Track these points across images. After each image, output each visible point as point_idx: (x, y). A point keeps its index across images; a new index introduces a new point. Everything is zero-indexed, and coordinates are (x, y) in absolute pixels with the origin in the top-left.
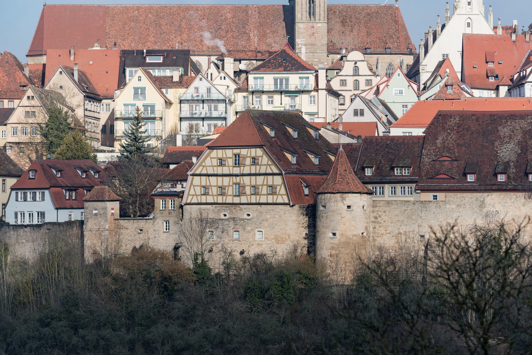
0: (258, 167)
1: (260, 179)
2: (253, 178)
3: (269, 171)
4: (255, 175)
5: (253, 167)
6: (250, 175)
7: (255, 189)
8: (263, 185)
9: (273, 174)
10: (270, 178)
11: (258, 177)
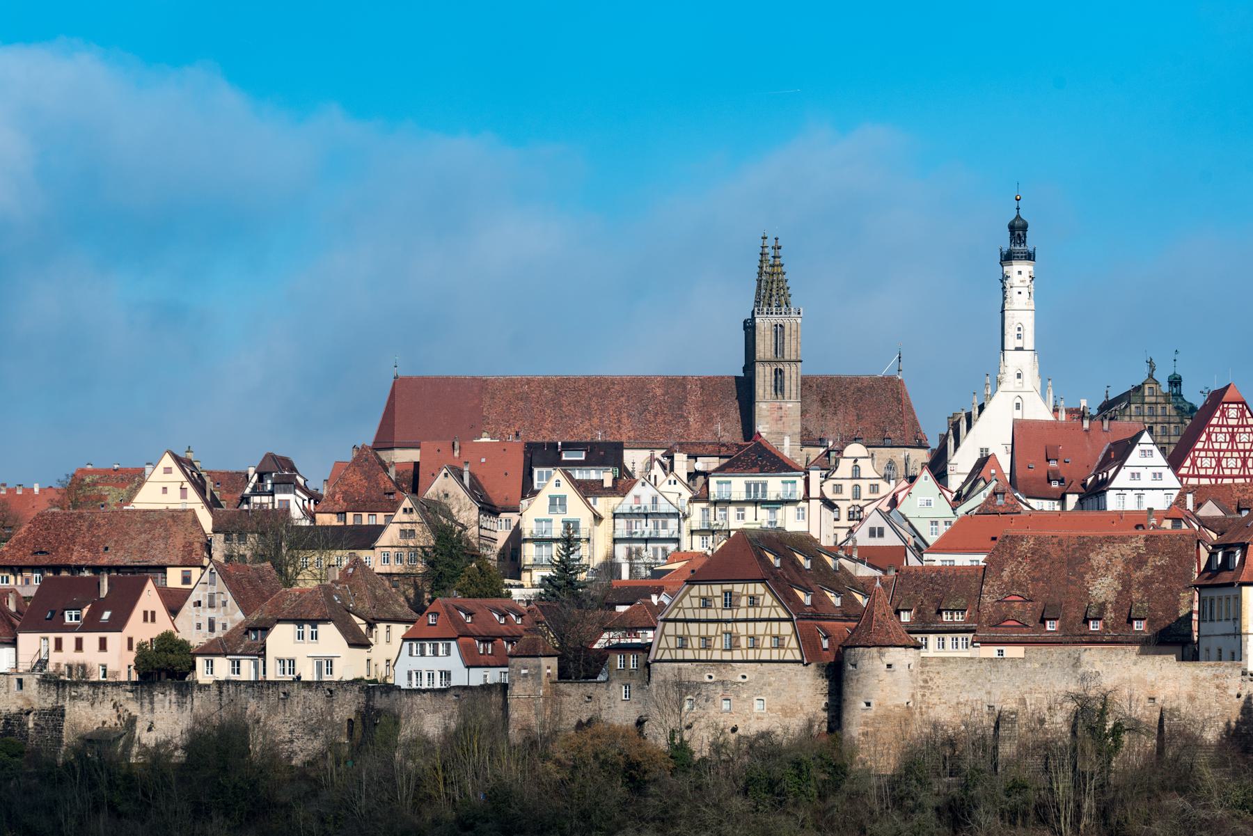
0: (758, 610)
1: (761, 627)
2: (751, 625)
3: (774, 615)
4: (754, 620)
5: (751, 610)
6: (746, 620)
7: (754, 641)
8: (764, 635)
9: (780, 620)
10: (775, 624)
11: (758, 624)
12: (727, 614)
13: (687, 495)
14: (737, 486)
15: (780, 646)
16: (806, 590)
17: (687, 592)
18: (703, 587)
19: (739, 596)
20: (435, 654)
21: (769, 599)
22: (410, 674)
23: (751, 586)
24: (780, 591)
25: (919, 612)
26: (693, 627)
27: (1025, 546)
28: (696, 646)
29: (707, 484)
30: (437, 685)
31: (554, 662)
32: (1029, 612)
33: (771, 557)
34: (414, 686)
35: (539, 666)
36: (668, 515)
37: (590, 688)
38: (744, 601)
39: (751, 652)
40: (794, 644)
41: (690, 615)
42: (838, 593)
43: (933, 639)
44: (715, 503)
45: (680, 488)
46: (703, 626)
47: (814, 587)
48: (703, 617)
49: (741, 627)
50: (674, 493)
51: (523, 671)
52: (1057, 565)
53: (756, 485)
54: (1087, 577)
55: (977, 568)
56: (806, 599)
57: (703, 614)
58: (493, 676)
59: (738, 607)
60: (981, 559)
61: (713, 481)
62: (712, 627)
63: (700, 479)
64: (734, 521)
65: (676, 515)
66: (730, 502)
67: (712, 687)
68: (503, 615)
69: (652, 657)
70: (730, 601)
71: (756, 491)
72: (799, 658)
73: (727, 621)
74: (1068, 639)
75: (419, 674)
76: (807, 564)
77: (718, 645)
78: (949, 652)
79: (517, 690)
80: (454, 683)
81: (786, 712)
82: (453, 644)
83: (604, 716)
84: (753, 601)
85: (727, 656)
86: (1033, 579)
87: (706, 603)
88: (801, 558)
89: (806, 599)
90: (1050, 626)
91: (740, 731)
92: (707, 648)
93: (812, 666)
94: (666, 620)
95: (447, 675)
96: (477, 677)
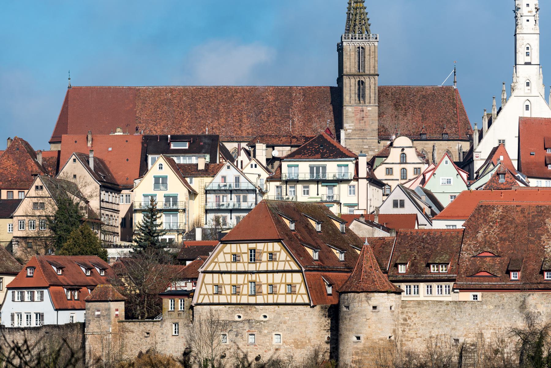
2: (270, 275)
5: (270, 264)
10: (289, 275)
12: (252, 267)
13: (265, 175)
14: (303, 169)
15: (292, 293)
16: (315, 249)
17: (222, 250)
18: (234, 246)
19: (261, 254)
20: (32, 300)
21: (283, 255)
22: (12, 316)
23: (270, 245)
24: (293, 248)
25: (412, 265)
26: (226, 277)
27: (496, 213)
28: (228, 292)
29: (280, 167)
30: (33, 325)
31: (121, 306)
32: (497, 265)
33: (287, 222)
34: (16, 325)
35: (109, 309)
36: (248, 191)
37: (149, 326)
38: (265, 257)
39: (270, 297)
40: (303, 290)
41: (223, 269)
42: (342, 251)
43: (423, 286)
44: (286, 182)
45: (259, 170)
46: (234, 276)
47: (323, 246)
48: (234, 269)
49: (263, 277)
50: (254, 174)
51: (97, 313)
52: (520, 229)
53: (318, 168)
54: (543, 238)
55: (458, 231)
56: (314, 255)
57: (233, 267)
58: (79, 317)
59: (261, 261)
60: (459, 225)
61: (284, 165)
62: (241, 277)
63: (277, 163)
64: (300, 196)
65: (254, 191)
66: (298, 181)
67: (241, 325)
68: (88, 269)
69: (195, 301)
70: (254, 256)
71: (318, 172)
72: (307, 301)
73: (252, 273)
74: (527, 286)
75: (20, 315)
76: (318, 228)
77: (245, 291)
78: (436, 296)
79: (91, 328)
80: (46, 322)
81: (298, 345)
82: (46, 292)
83: (159, 348)
84: (272, 257)
85: (252, 300)
86: (501, 239)
87: (236, 258)
88: (313, 223)
89: (314, 255)
90: (513, 276)
91: (261, 361)
92: (237, 293)
93: (318, 308)
94: (205, 272)
95: (40, 316)
96: (64, 318)
